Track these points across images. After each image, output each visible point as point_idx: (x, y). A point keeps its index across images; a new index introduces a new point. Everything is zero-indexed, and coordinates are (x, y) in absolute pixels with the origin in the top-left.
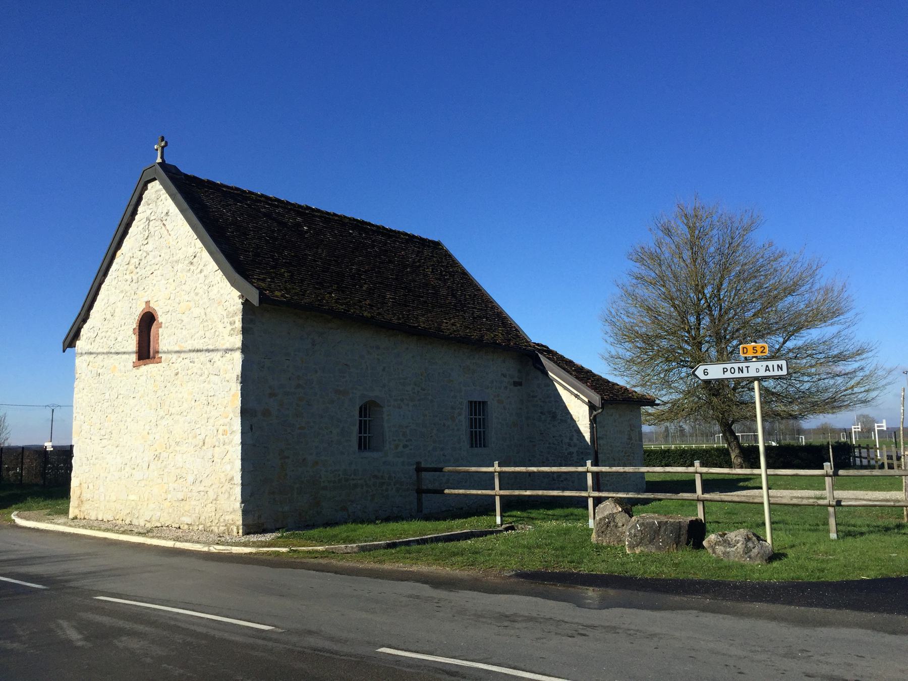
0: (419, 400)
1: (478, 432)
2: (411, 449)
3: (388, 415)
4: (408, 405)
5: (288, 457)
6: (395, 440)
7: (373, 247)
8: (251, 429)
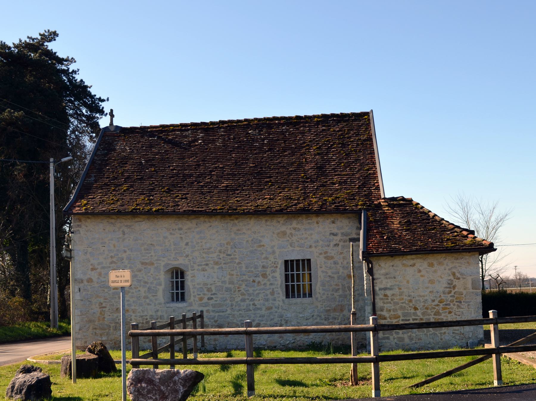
0: (225, 263)
1: (296, 285)
2: (216, 301)
3: (192, 277)
4: (213, 268)
5: (105, 307)
6: (200, 295)
7: (263, 140)
8: (80, 291)
